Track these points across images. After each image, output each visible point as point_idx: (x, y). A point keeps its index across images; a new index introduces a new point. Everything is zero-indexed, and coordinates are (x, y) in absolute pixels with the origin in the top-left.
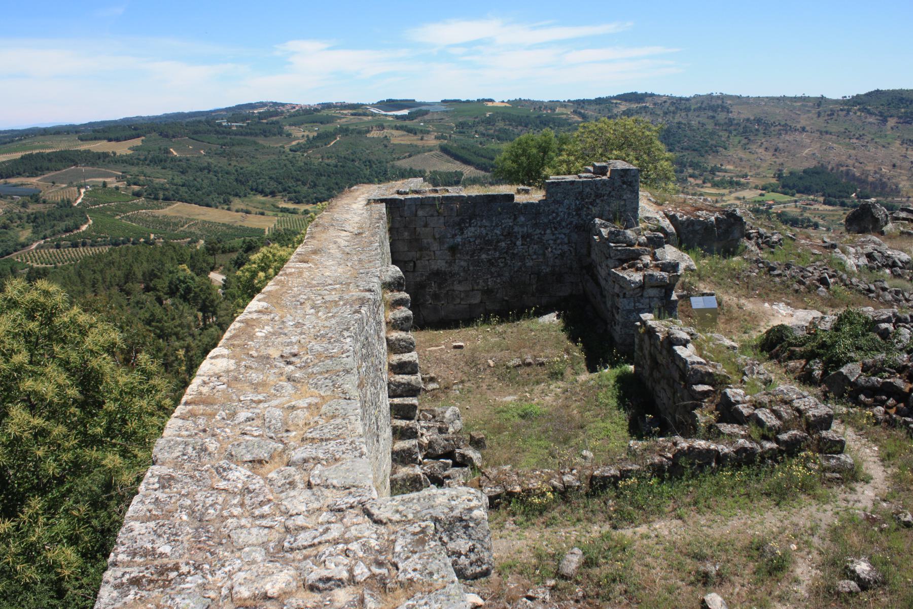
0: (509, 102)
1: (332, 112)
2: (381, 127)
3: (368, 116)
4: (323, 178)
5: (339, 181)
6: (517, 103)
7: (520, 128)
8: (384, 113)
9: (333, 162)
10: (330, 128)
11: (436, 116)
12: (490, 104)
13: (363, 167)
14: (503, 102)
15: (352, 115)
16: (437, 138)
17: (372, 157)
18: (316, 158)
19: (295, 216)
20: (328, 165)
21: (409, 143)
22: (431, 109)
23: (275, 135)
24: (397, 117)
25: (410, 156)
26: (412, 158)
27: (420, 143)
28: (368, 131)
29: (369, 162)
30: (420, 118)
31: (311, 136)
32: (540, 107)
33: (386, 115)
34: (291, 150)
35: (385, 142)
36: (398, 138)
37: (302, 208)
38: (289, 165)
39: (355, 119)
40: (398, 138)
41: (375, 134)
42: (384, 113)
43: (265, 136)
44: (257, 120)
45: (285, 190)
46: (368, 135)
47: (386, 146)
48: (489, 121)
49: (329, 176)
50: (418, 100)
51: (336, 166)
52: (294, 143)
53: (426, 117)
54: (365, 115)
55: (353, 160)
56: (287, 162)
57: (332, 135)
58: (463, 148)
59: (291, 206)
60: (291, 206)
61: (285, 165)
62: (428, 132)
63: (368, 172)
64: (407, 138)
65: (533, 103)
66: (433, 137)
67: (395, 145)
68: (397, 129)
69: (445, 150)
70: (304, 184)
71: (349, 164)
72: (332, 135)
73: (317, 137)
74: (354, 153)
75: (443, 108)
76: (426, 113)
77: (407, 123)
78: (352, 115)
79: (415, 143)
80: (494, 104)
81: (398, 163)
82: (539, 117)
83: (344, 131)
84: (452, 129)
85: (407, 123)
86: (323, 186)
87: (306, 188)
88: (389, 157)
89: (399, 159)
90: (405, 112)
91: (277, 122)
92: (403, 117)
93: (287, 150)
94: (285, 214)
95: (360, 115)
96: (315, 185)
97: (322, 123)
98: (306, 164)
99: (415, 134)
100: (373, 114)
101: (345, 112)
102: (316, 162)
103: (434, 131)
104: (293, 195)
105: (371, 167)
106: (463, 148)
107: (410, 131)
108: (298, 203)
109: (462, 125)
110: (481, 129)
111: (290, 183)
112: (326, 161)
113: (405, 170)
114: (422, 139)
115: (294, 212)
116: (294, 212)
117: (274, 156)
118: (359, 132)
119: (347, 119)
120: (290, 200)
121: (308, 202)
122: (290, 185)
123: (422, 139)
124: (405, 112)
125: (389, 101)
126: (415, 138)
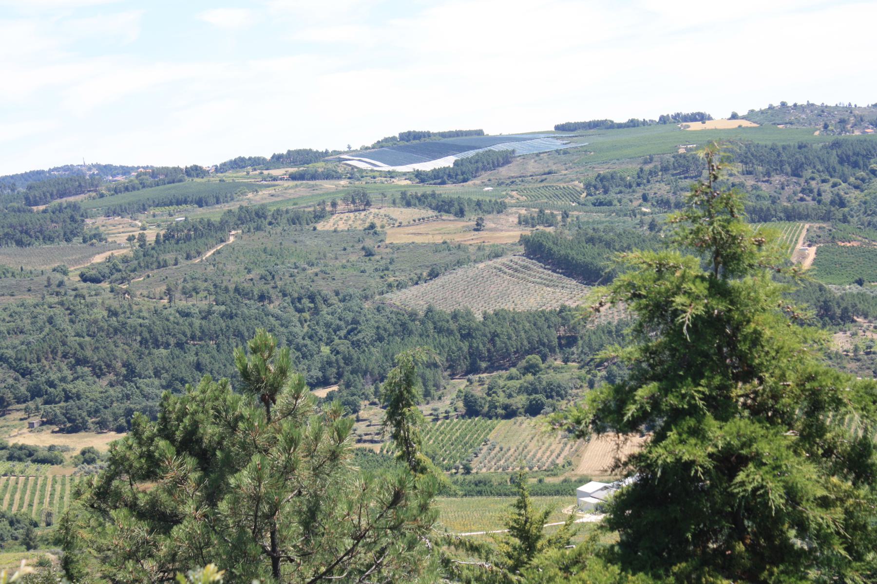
0: (751, 115)
1: (239, 176)
2: (360, 200)
3: (339, 178)
4: (163, 351)
5: (205, 359)
6: (779, 114)
7: (777, 179)
8: (386, 168)
9: (198, 304)
10: (214, 213)
11: (532, 167)
12: (695, 126)
13: (295, 316)
14: (734, 116)
15: (293, 177)
16: (523, 221)
17: (325, 288)
18: (146, 296)
19: (48, 470)
20: (186, 315)
21: (439, 239)
22: (520, 148)
23: (50, 239)
24: (420, 177)
25: (433, 275)
26: (438, 281)
27: (471, 239)
28: (319, 216)
29: (312, 298)
30: (485, 176)
31: (151, 235)
32: (843, 122)
33: (391, 175)
34: (84, 278)
35: (369, 243)
36: (410, 230)
37: (77, 443)
38: (63, 320)
39: (300, 189)
40: (410, 230)
41: (341, 221)
42: (386, 168)
43: (20, 243)
44: (21, 204)
45: (36, 393)
46: (320, 226)
47: (369, 254)
48: (683, 166)
49: (180, 345)
50: (490, 131)
51: (206, 315)
52: (98, 259)
53: (504, 172)
54: (329, 176)
55: (262, 298)
56: (59, 310)
57: (213, 231)
58: (591, 240)
59: (42, 440)
60: (42, 440)
61: (50, 320)
62: (500, 208)
63: (300, 331)
64: (438, 225)
65: (823, 111)
66: (514, 219)
67: (398, 248)
68: (408, 204)
69: (536, 250)
70: (98, 373)
71: (251, 308)
72: (213, 231)
73: (167, 237)
74: (269, 276)
75: (558, 145)
76: (506, 159)
77: (450, 190)
78: (293, 177)
79: (458, 239)
80: (709, 125)
81: (396, 298)
82: (836, 145)
83: (254, 219)
84: (573, 195)
85: (450, 190)
86: (157, 374)
87: (104, 382)
88: (375, 283)
89: (400, 286)
90: (447, 162)
91: (75, 207)
92: (440, 177)
93: (74, 278)
94: (18, 466)
95: (314, 177)
96: (131, 373)
97: (200, 203)
98: (113, 313)
99: (461, 213)
100: (353, 174)
101: (275, 172)
102: (148, 305)
103: (519, 205)
104: (57, 409)
105: (316, 311)
106: (591, 240)
107: (444, 207)
108: (74, 427)
109: (604, 182)
110: (661, 189)
111: (57, 371)
112: (182, 303)
113: (413, 316)
114: (479, 227)
115: (49, 459)
116: (49, 459)
117: (30, 299)
118: (296, 220)
119: (285, 193)
120: (49, 422)
121: (102, 427)
122: (54, 376)
123: (479, 227)
124: (447, 162)
125: (408, 137)
126: (461, 224)
